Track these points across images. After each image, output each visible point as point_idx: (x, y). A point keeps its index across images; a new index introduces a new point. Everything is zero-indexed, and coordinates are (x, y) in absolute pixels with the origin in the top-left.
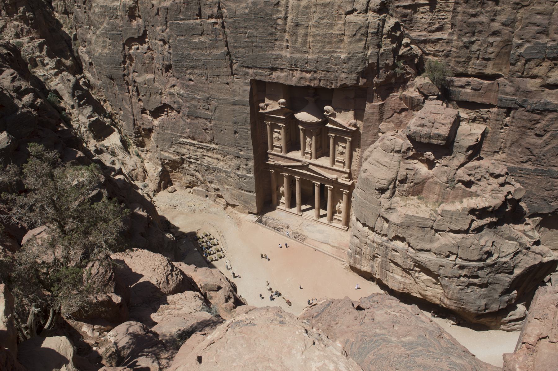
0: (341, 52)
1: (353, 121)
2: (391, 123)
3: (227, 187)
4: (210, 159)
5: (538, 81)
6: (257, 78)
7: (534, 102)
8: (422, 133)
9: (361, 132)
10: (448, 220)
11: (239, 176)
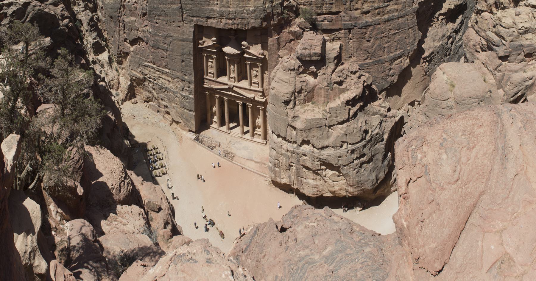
1: (261, 51)
5: (359, 11)
6: (198, 23)
7: (360, 23)
8: (306, 54)
9: (267, 58)
10: (335, 115)
11: (183, 96)
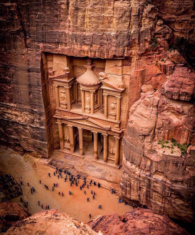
0: (111, 31)
2: (150, 85)
3: (24, 137)
4: (9, 116)
6: (46, 51)
